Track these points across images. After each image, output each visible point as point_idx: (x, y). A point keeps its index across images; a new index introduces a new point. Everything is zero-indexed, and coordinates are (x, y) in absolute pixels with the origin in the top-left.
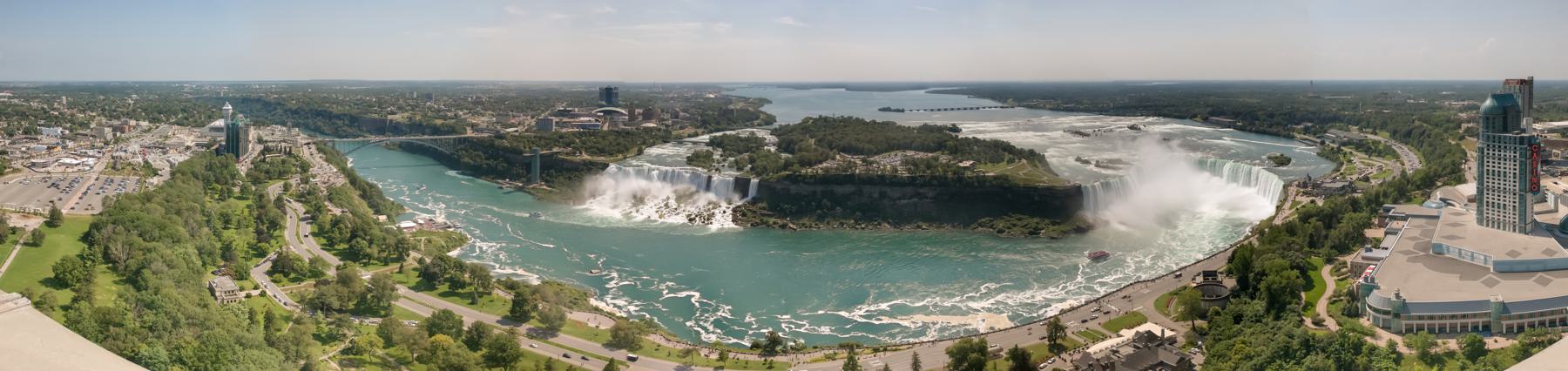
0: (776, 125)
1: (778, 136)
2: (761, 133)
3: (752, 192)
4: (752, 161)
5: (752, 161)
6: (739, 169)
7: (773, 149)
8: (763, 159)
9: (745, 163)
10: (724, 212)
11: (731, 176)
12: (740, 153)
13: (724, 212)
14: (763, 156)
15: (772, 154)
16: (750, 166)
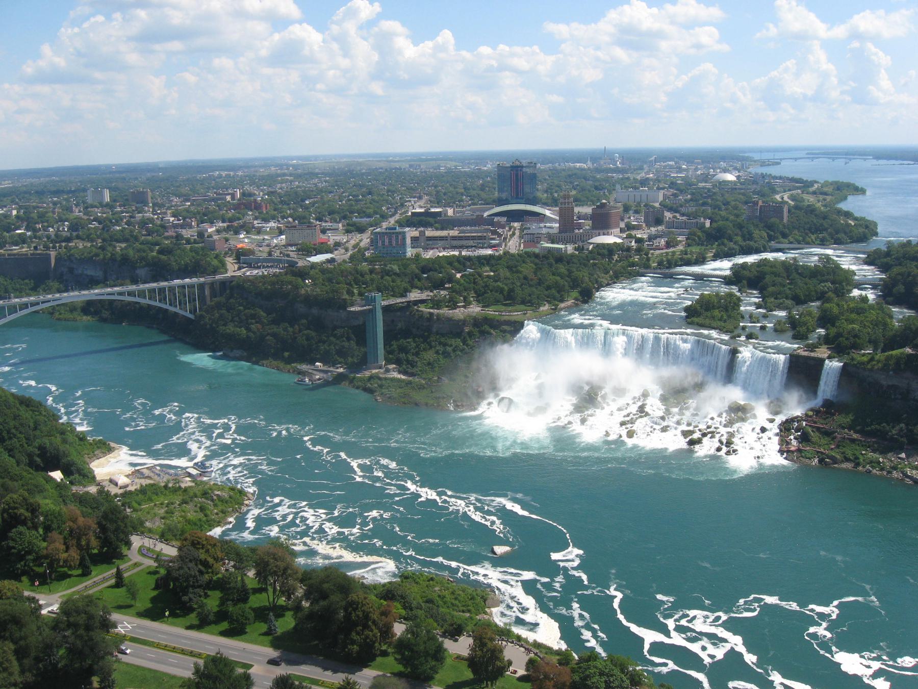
0: (879, 242)
1: (884, 268)
2: (847, 261)
3: (827, 387)
4: (825, 320)
5: (825, 320)
6: (798, 337)
7: (871, 296)
8: (853, 316)
9: (811, 322)
10: (763, 430)
11: (779, 350)
12: (799, 301)
13: (763, 430)
14: (852, 311)
15: (871, 307)
16: (822, 331)
